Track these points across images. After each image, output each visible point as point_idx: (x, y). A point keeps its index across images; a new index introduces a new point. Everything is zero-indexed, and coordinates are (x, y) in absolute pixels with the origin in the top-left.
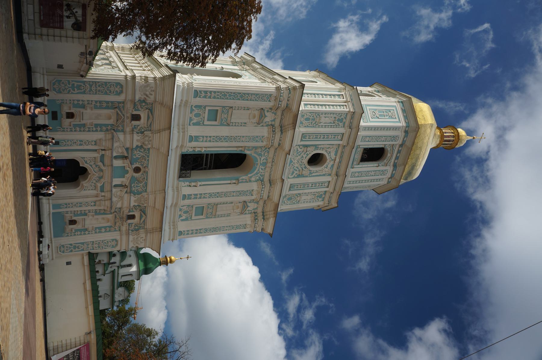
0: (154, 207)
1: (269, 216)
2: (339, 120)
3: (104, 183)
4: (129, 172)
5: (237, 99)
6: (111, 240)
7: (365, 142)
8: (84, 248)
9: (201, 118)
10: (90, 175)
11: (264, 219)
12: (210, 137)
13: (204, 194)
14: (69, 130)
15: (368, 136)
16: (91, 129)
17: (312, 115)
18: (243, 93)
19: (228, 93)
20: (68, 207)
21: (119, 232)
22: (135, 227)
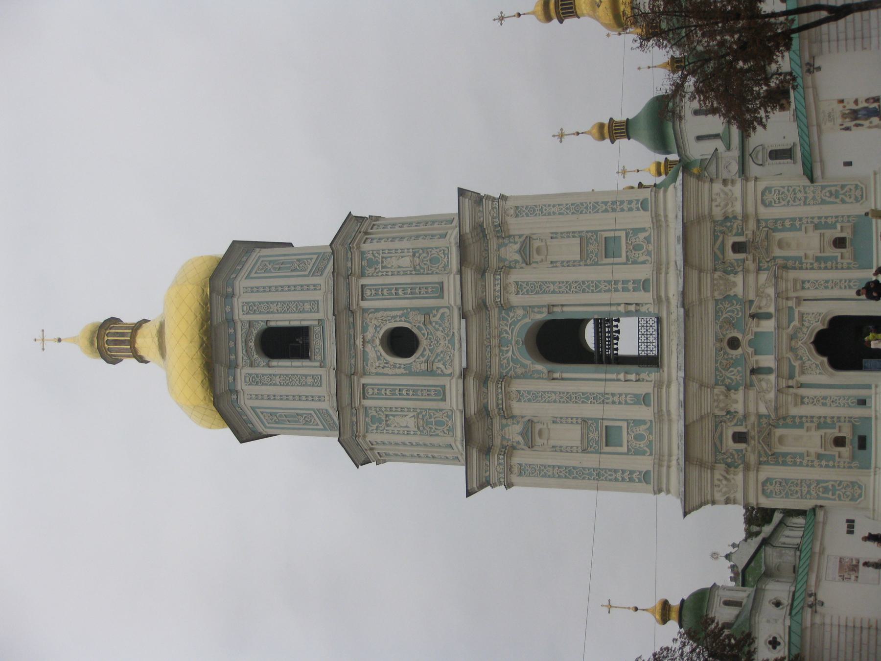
0: (700, 271)
1: (473, 235)
3: (789, 327)
4: (747, 343)
5: (579, 468)
6: (773, 204)
7: (313, 376)
8: (821, 191)
9: (633, 432)
10: (812, 340)
11: (481, 226)
12: (614, 403)
13: (609, 291)
14: (842, 420)
15: (310, 385)
16: (809, 420)
17: (434, 432)
18: (569, 478)
19: (594, 479)
20: (847, 281)
21: (760, 218)
22: (731, 226)
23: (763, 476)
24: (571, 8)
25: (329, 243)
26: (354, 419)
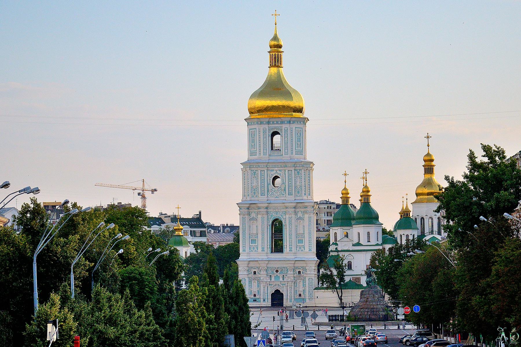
0: (294, 264)
2: (254, 175)
11: (307, 208)
13: (290, 241)
15: (264, 151)
23: (245, 278)
24: (427, 173)
26: (255, 166)
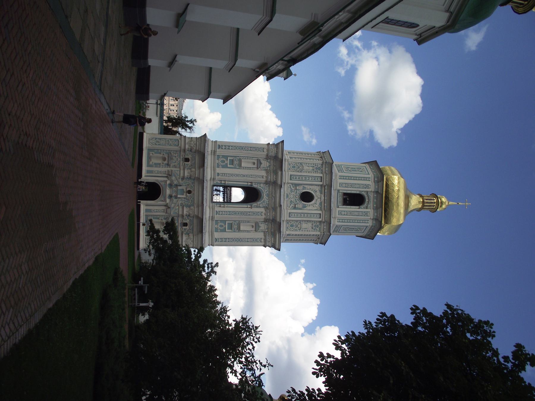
7: (342, 187)
15: (344, 183)
25: (331, 235)
